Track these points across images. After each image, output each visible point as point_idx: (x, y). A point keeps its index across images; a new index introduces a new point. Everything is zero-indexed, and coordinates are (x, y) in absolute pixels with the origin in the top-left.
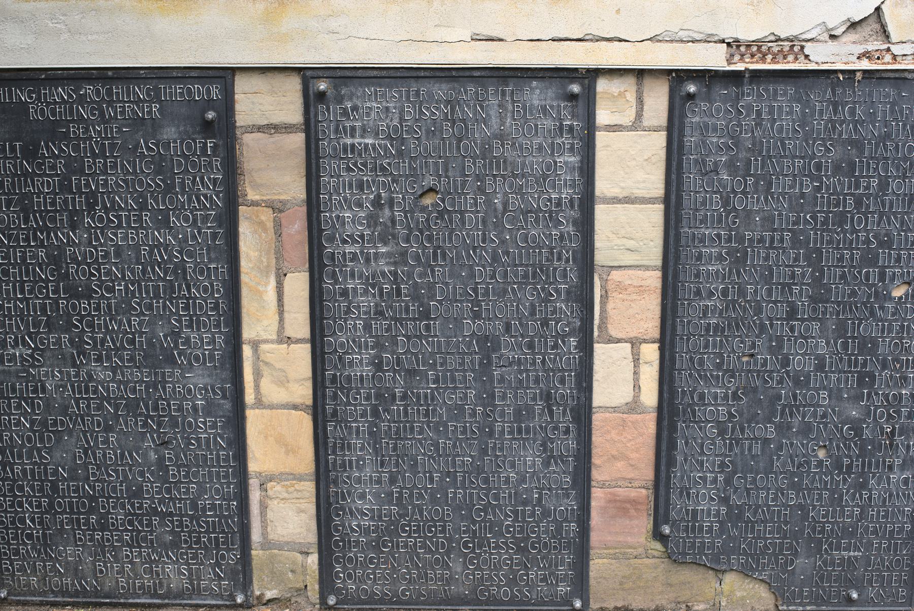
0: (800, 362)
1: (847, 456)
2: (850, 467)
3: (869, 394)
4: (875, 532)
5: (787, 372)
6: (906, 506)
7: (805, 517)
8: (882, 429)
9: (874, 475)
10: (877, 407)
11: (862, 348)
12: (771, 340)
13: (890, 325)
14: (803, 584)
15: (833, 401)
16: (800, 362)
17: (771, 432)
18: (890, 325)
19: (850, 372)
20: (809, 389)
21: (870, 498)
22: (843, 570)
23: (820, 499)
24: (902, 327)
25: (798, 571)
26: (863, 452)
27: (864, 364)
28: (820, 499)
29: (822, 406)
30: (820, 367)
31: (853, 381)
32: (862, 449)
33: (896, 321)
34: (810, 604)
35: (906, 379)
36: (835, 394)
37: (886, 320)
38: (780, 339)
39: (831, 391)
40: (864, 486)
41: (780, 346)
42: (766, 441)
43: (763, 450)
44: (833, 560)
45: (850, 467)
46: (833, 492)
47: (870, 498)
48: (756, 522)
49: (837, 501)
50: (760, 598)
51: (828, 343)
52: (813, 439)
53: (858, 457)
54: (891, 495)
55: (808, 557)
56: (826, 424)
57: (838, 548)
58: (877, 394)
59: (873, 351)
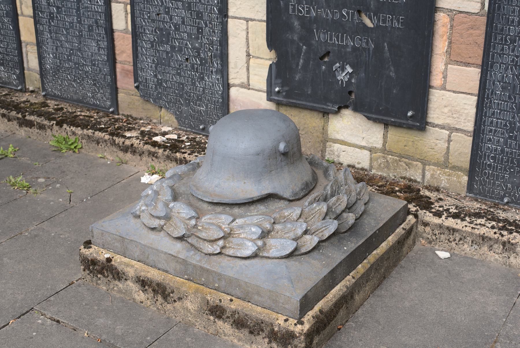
0: (177, 20)
1: (196, 64)
2: (197, 68)
3: (201, 37)
4: (208, 100)
5: (172, 23)
6: (219, 91)
7: (183, 89)
8: (207, 54)
9: (206, 74)
10: (205, 44)
11: (198, 17)
12: (166, 9)
13: (207, 7)
14: (186, 118)
15: (189, 39)
16: (177, 20)
17: (169, 49)
18: (207, 7)
19: (194, 26)
20: (180, 32)
21: (205, 84)
22: (198, 115)
23: (188, 82)
24: (211, 8)
25: (183, 112)
26: (201, 64)
27: (199, 24)
28: (188, 82)
29: (185, 40)
30: (183, 22)
31: (195, 31)
32: (201, 61)
33: (209, 5)
34: (188, 127)
35: (214, 32)
36: (190, 35)
37: (205, 5)
38: (168, 8)
39: (188, 33)
40: (203, 79)
41: (169, 11)
42: (167, 53)
43: (167, 56)
44: (194, 109)
45: (197, 68)
46: (192, 79)
47: (205, 84)
48: (167, 87)
49: (194, 84)
50: (173, 121)
51: (185, 12)
52: (183, 54)
53: (200, 65)
54: (213, 85)
55: (186, 107)
56: (187, 49)
57: (196, 105)
58: (204, 38)
59: (201, 18)
